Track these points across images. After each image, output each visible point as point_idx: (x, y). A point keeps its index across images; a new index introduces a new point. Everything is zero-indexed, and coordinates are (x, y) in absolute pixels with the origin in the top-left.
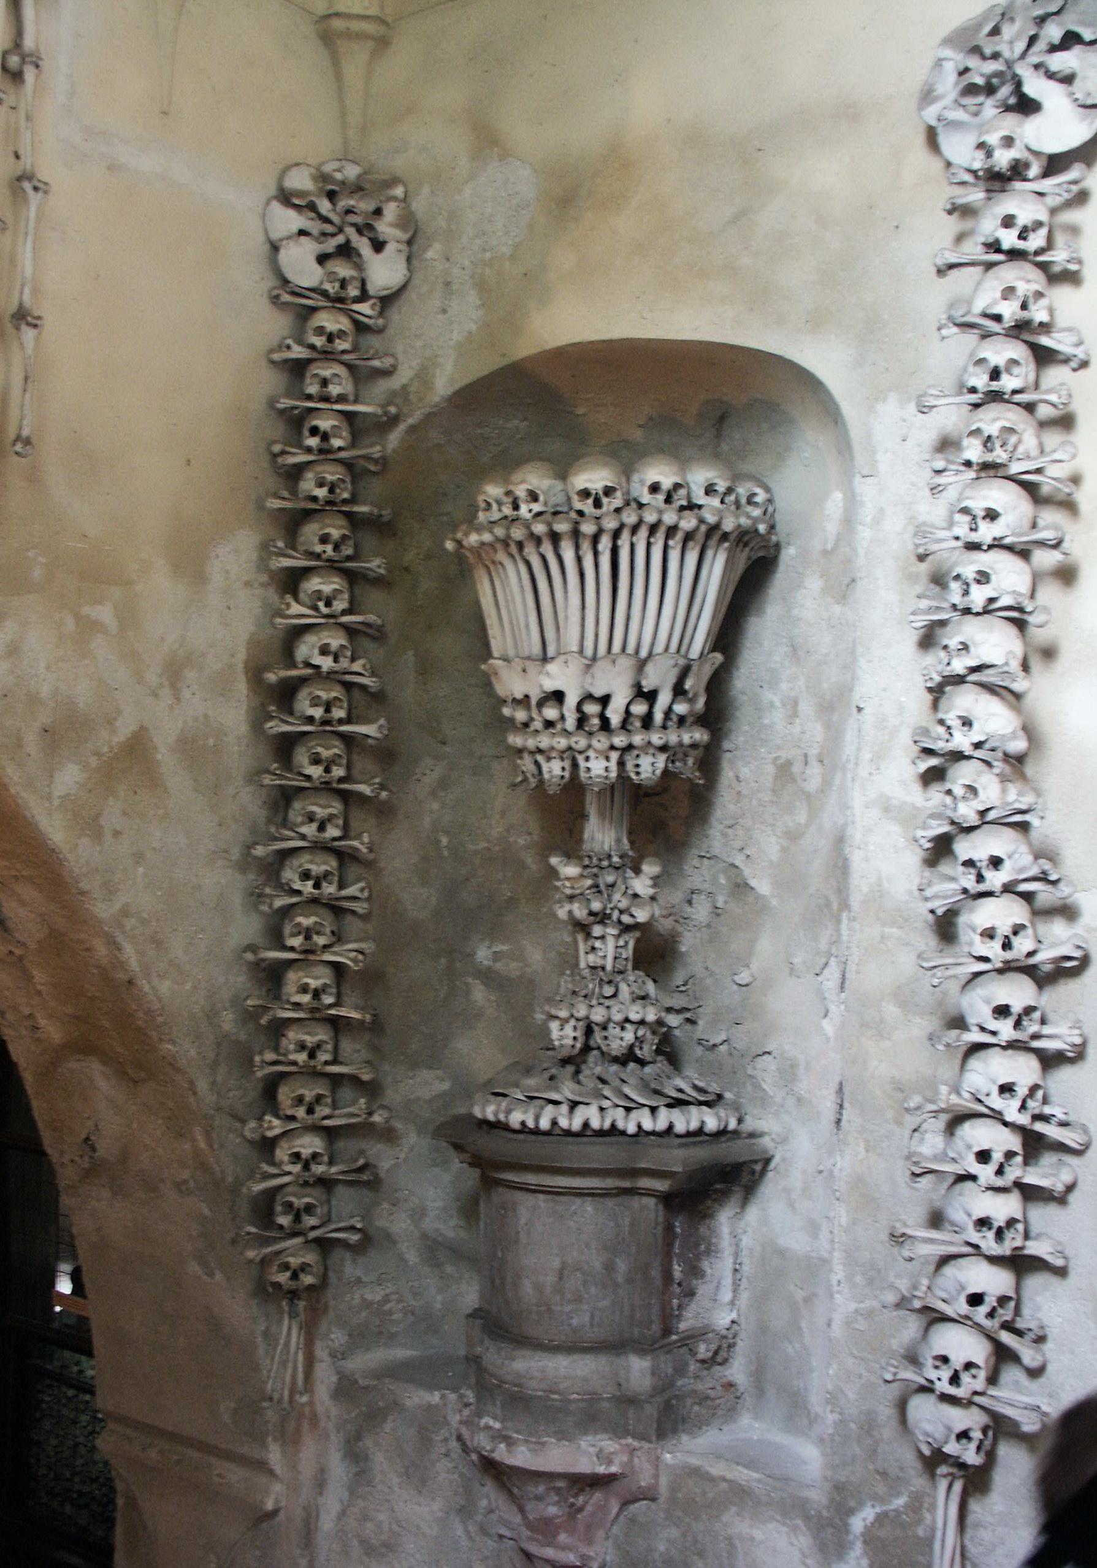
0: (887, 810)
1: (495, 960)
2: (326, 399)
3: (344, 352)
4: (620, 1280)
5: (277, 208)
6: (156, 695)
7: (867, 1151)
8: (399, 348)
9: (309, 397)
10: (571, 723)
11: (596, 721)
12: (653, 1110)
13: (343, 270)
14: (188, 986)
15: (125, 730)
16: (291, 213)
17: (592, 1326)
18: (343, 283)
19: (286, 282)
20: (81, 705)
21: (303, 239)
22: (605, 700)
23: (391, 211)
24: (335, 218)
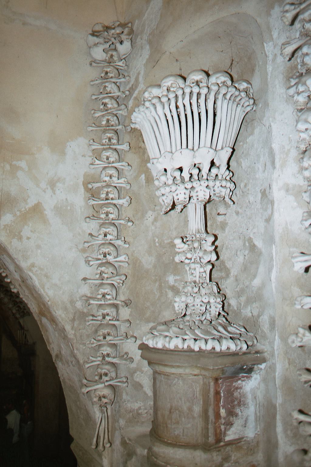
0: (287, 190)
1: (175, 282)
4: (196, 415)
6: (45, 192)
7: (289, 364)
10: (170, 182)
11: (178, 178)
12: (206, 341)
14: (61, 292)
15: (32, 202)
17: (183, 435)
20: (13, 194)
22: (181, 169)
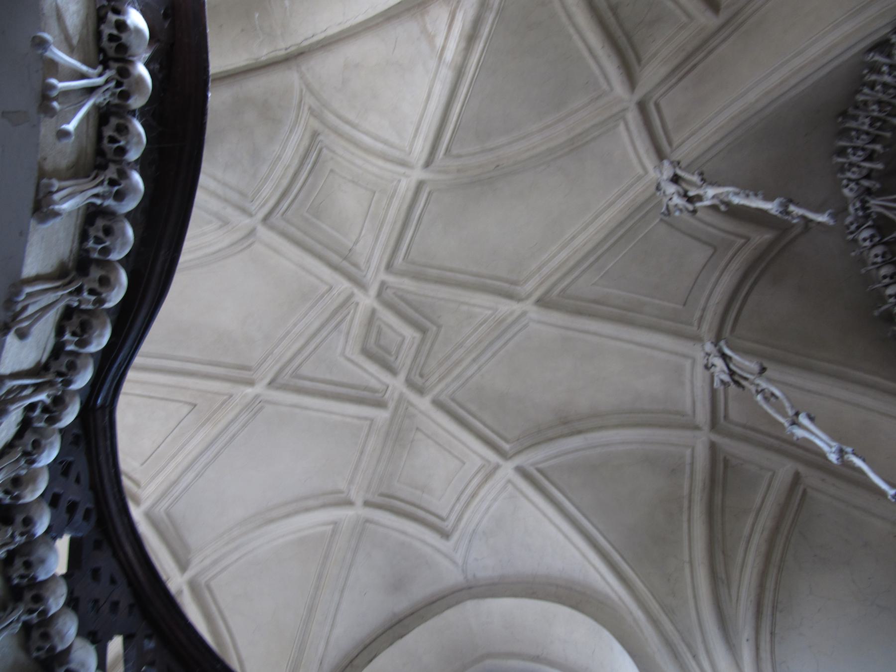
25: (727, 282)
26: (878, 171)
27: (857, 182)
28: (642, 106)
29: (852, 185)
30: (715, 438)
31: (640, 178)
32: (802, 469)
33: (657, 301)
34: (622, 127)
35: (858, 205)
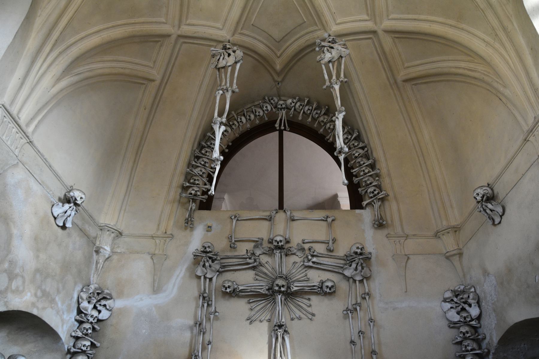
2: (467, 351)
3: (469, 336)
5: (443, 303)
8: (485, 332)
9: (464, 351)
13: (464, 314)
16: (447, 304)
18: (465, 318)
19: (451, 321)
21: (452, 310)
23: (471, 296)
24: (458, 302)
25: (261, 48)
26: (298, 117)
27: (295, 106)
28: (374, 32)
29: (293, 104)
30: (174, 37)
31: (335, 20)
32: (157, 83)
33: (258, 10)
34: (366, 17)
35: (284, 106)
